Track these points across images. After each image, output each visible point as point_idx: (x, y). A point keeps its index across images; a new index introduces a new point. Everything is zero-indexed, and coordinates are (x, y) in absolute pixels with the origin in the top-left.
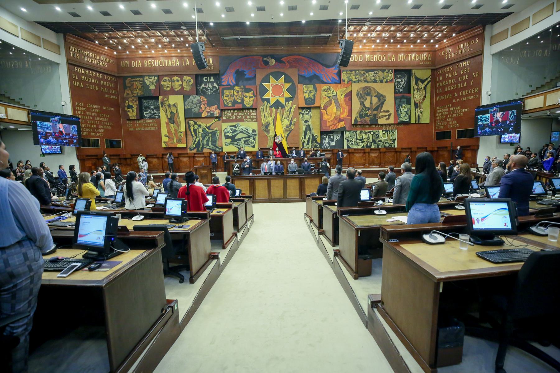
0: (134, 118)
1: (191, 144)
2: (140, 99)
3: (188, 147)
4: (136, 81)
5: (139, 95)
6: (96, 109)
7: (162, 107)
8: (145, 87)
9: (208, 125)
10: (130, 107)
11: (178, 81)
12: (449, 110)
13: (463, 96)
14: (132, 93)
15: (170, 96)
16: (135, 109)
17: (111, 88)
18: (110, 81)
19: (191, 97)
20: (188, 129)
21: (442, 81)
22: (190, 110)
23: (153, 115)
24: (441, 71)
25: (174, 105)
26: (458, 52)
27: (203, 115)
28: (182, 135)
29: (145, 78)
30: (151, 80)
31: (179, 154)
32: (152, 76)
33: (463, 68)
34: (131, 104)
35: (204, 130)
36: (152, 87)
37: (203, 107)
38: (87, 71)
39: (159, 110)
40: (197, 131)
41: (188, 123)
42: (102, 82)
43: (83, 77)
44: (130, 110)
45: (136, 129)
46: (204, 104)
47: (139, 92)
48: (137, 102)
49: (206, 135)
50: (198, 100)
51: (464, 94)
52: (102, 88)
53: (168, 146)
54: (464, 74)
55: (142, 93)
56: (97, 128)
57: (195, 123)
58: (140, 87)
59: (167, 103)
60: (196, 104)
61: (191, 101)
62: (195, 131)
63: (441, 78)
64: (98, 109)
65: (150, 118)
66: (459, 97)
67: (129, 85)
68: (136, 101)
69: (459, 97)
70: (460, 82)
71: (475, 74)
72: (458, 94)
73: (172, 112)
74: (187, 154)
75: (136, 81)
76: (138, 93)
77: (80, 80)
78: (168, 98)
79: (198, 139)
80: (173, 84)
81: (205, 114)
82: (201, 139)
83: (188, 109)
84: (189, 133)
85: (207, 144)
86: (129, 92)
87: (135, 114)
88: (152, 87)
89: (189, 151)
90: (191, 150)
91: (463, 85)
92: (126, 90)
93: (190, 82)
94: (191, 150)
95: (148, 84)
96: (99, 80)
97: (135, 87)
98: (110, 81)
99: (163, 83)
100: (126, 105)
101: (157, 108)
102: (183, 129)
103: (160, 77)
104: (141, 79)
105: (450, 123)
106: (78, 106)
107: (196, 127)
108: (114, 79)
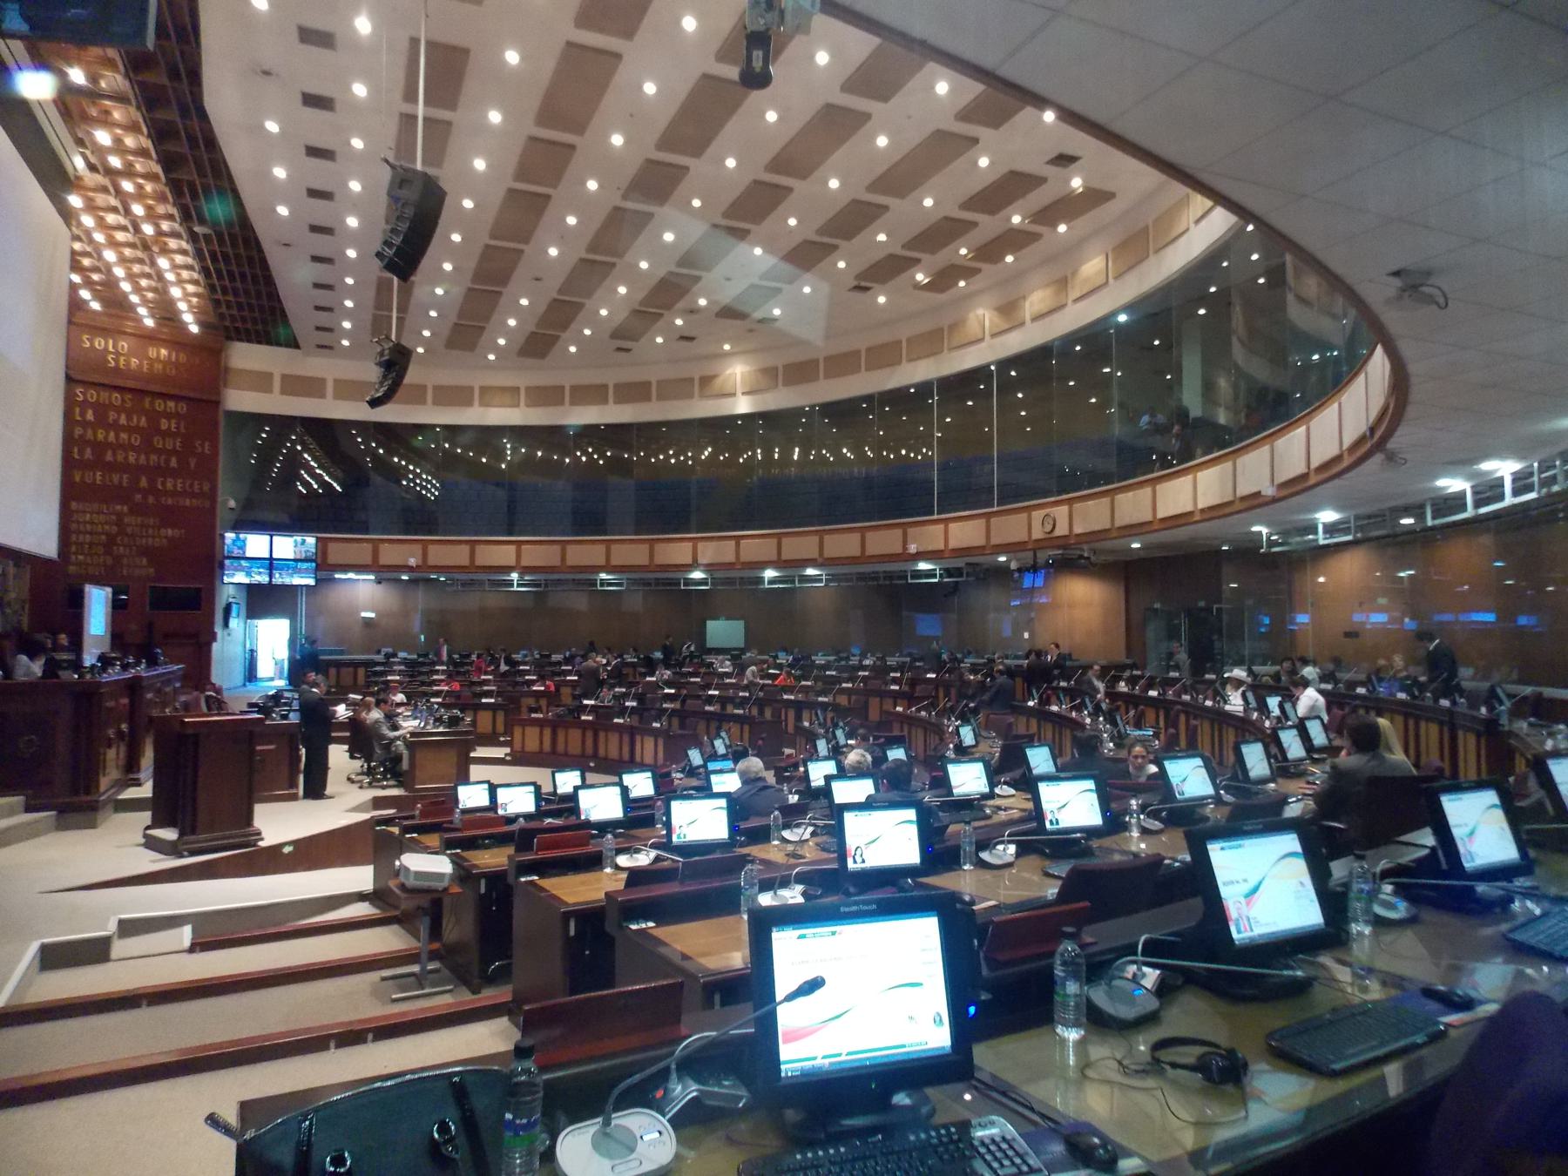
12: (119, 523)
13: (166, 493)
21: (93, 426)
24: (92, 396)
26: (151, 365)
33: (169, 416)
51: (169, 485)
54: (166, 434)
63: (90, 416)
66: (152, 490)
69: (152, 490)
70: (159, 452)
71: (202, 446)
72: (152, 481)
91: (167, 461)
105: (125, 561)
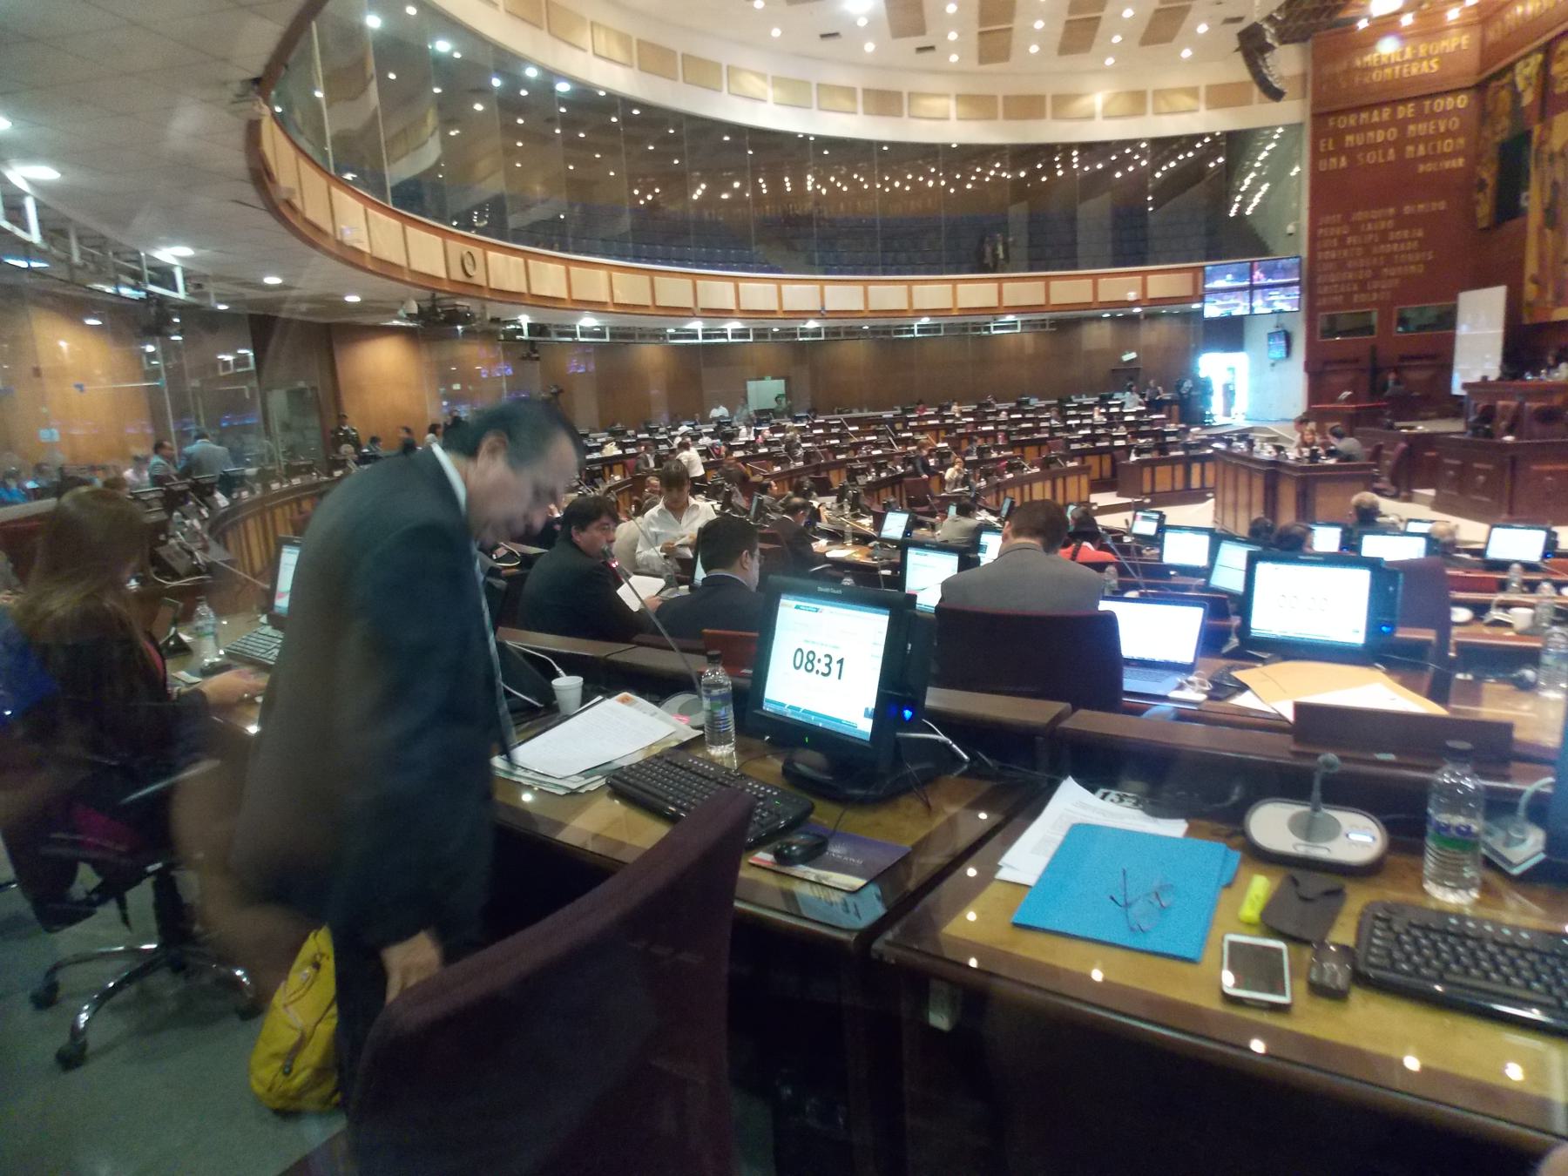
0: (1484, 224)
8: (1517, 96)
10: (1482, 185)
16: (1489, 191)
17: (1449, 133)
30: (1527, 71)
36: (1528, 98)
43: (1349, 139)
44: (1480, 196)
52: (1410, 149)
59: (1546, 148)
64: (1386, 218)
77: (1340, 150)
88: (1528, 98)
98: (1445, 114)
100: (1476, 181)
103: (1548, 50)
108: (1462, 101)
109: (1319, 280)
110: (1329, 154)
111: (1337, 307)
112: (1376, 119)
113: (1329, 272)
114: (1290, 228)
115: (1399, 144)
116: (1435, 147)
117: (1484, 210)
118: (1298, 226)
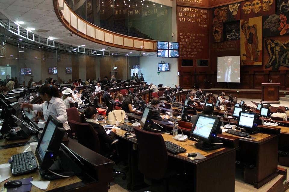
0: (219, 41)
1: (268, 62)
2: (225, 24)
3: (264, 65)
4: (222, 10)
5: (224, 21)
6: (193, 36)
7: (242, 29)
8: (229, 13)
9: (286, 43)
10: (216, 32)
11: (258, 4)
14: (219, 20)
15: (249, 19)
16: (220, 34)
18: (203, 14)
19: (270, 17)
20: (265, 48)
22: (269, 29)
23: (234, 37)
25: (253, 26)
27: (281, 33)
28: (259, 54)
29: (229, 7)
30: (234, 7)
31: (255, 72)
32: (235, 3)
34: (217, 29)
35: (281, 48)
37: (282, 25)
38: (188, 9)
39: (240, 33)
40: (274, 49)
41: (266, 42)
42: (198, 15)
43: (185, 14)
44: (216, 34)
45: (220, 50)
46: (283, 22)
47: (224, 19)
48: (222, 27)
49: (284, 53)
50: (278, 19)
52: (197, 20)
53: (245, 65)
55: (227, 20)
56: (192, 51)
57: (273, 42)
58: (225, 14)
59: (246, 25)
60: (275, 23)
61: (270, 21)
62: (272, 49)
65: (232, 39)
67: (217, 14)
68: (221, 27)
73: (251, 34)
74: (263, 72)
75: (222, 10)
76: (223, 20)
77: (183, 17)
78: (248, 21)
79: (274, 57)
80: (253, 7)
81: (283, 32)
82: (278, 57)
83: (266, 29)
84: (266, 51)
85: (284, 62)
86: (216, 20)
87: (220, 37)
88: (235, 13)
89: (264, 69)
90: (266, 67)
92: (214, 19)
93: (270, 2)
94: (266, 67)
95: (231, 11)
96: (196, 13)
97: (221, 15)
98: (203, 14)
99: (244, 8)
100: (214, 31)
101: (238, 31)
102: (260, 48)
104: (226, 8)
106: (181, 35)
107: (273, 45)
109: (181, 49)
110: (181, 17)
111: (184, 57)
112: (190, 11)
113: (183, 48)
114: (173, 35)
115: (196, 18)
116: (202, 21)
117: (218, 38)
118: (174, 34)
